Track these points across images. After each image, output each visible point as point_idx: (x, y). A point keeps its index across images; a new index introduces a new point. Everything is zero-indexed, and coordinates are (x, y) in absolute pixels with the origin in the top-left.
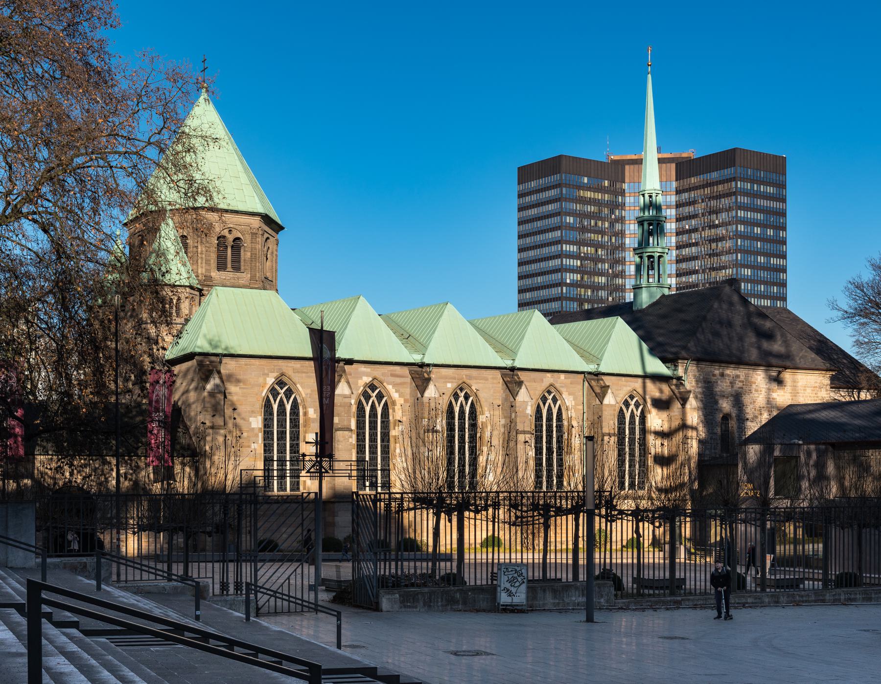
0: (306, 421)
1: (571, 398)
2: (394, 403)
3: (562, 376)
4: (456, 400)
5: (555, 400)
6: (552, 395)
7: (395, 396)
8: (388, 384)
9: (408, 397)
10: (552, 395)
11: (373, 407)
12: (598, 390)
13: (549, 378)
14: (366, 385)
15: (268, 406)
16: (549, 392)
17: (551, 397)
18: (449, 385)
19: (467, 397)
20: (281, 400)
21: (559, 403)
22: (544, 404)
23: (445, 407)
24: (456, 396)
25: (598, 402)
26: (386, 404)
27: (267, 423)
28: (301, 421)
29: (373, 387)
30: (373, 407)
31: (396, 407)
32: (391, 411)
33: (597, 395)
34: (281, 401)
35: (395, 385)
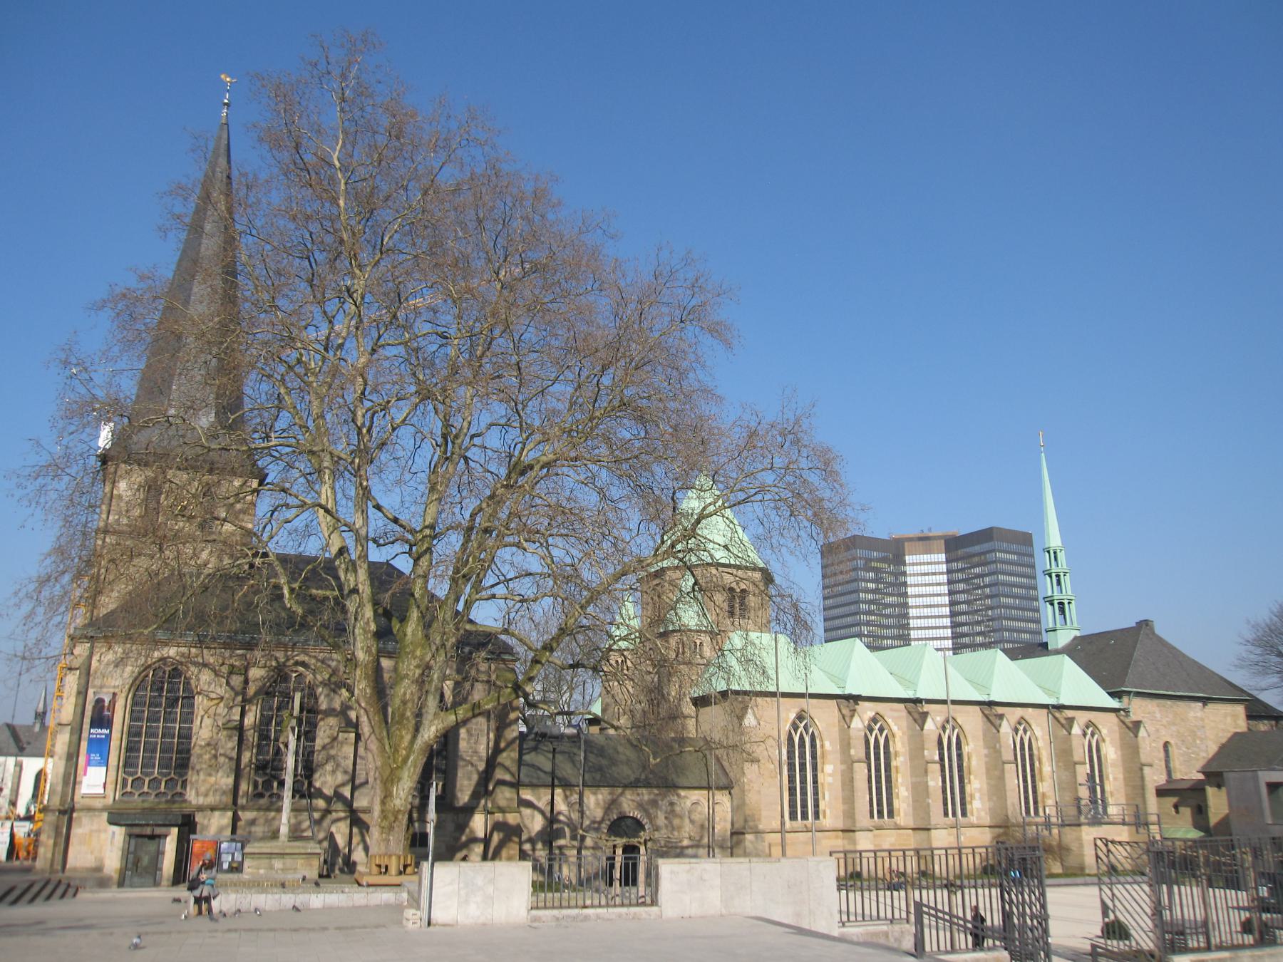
0: (823, 754)
1: (1039, 728)
2: (893, 735)
3: (1030, 710)
5: (1025, 731)
7: (895, 728)
9: (905, 729)
11: (876, 740)
12: (1063, 721)
13: (1019, 712)
16: (1020, 723)
17: (1021, 728)
18: (938, 718)
21: (1028, 733)
23: (936, 738)
24: (944, 728)
25: (1065, 732)
26: (887, 737)
29: (874, 720)
30: (876, 740)
32: (891, 743)
33: (1063, 726)
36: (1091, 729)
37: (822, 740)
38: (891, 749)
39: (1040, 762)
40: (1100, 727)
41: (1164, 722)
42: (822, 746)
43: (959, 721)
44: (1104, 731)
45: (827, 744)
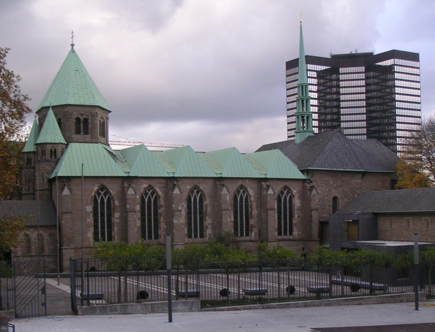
0: (114, 207)
2: (159, 197)
4: (192, 194)
6: (243, 190)
8: (156, 188)
10: (243, 190)
14: (145, 189)
15: (95, 200)
16: (241, 189)
19: (197, 193)
20: (102, 197)
22: (238, 194)
24: (192, 191)
26: (156, 197)
27: (95, 209)
28: (112, 207)
31: (160, 199)
32: (158, 200)
34: (102, 197)
35: (159, 188)
36: (286, 191)
37: (113, 200)
38: (158, 204)
39: (252, 209)
40: (292, 189)
41: (335, 185)
42: (114, 203)
43: (201, 188)
44: (295, 192)
45: (117, 203)
